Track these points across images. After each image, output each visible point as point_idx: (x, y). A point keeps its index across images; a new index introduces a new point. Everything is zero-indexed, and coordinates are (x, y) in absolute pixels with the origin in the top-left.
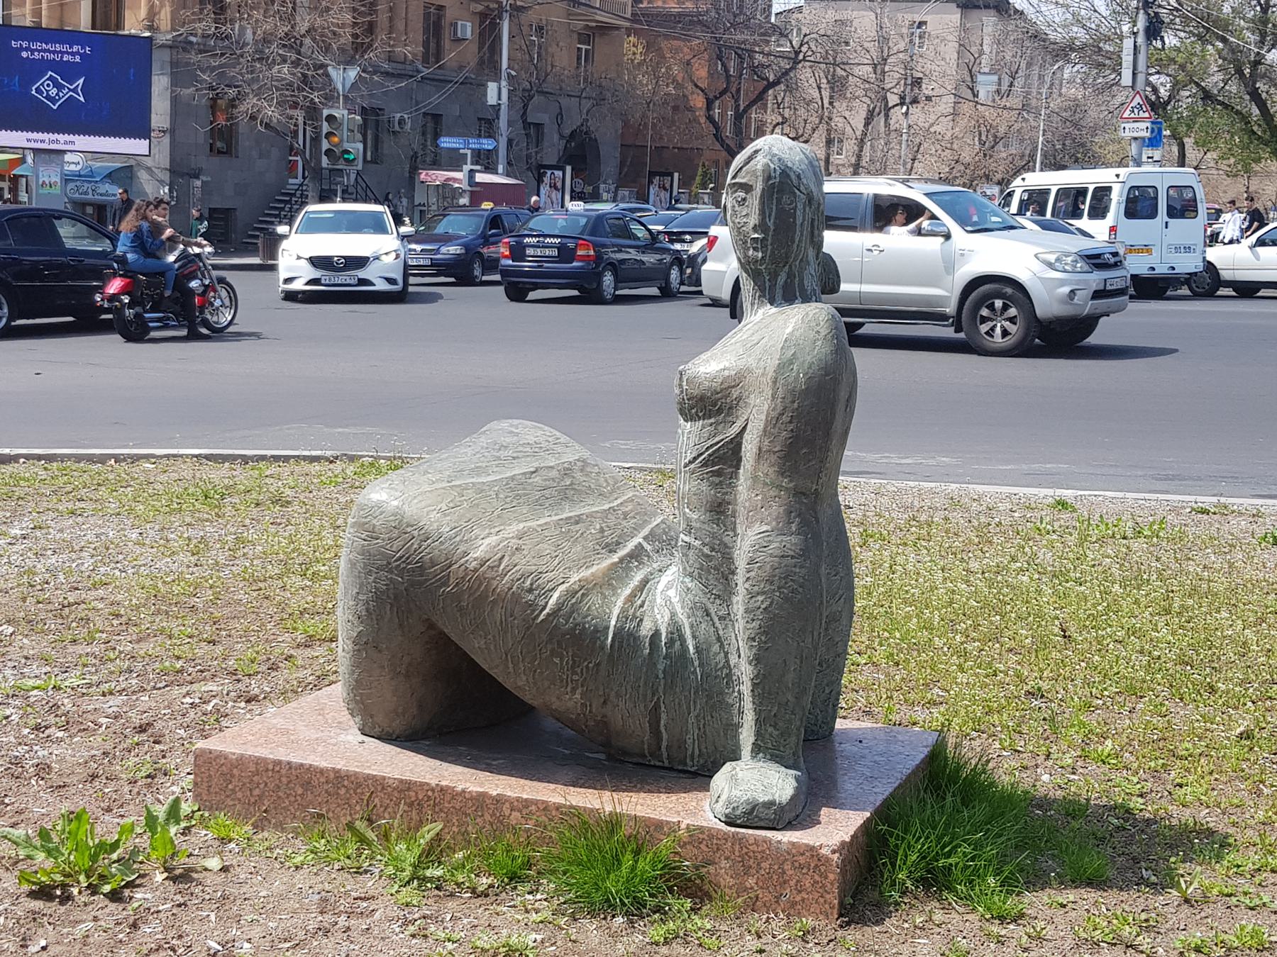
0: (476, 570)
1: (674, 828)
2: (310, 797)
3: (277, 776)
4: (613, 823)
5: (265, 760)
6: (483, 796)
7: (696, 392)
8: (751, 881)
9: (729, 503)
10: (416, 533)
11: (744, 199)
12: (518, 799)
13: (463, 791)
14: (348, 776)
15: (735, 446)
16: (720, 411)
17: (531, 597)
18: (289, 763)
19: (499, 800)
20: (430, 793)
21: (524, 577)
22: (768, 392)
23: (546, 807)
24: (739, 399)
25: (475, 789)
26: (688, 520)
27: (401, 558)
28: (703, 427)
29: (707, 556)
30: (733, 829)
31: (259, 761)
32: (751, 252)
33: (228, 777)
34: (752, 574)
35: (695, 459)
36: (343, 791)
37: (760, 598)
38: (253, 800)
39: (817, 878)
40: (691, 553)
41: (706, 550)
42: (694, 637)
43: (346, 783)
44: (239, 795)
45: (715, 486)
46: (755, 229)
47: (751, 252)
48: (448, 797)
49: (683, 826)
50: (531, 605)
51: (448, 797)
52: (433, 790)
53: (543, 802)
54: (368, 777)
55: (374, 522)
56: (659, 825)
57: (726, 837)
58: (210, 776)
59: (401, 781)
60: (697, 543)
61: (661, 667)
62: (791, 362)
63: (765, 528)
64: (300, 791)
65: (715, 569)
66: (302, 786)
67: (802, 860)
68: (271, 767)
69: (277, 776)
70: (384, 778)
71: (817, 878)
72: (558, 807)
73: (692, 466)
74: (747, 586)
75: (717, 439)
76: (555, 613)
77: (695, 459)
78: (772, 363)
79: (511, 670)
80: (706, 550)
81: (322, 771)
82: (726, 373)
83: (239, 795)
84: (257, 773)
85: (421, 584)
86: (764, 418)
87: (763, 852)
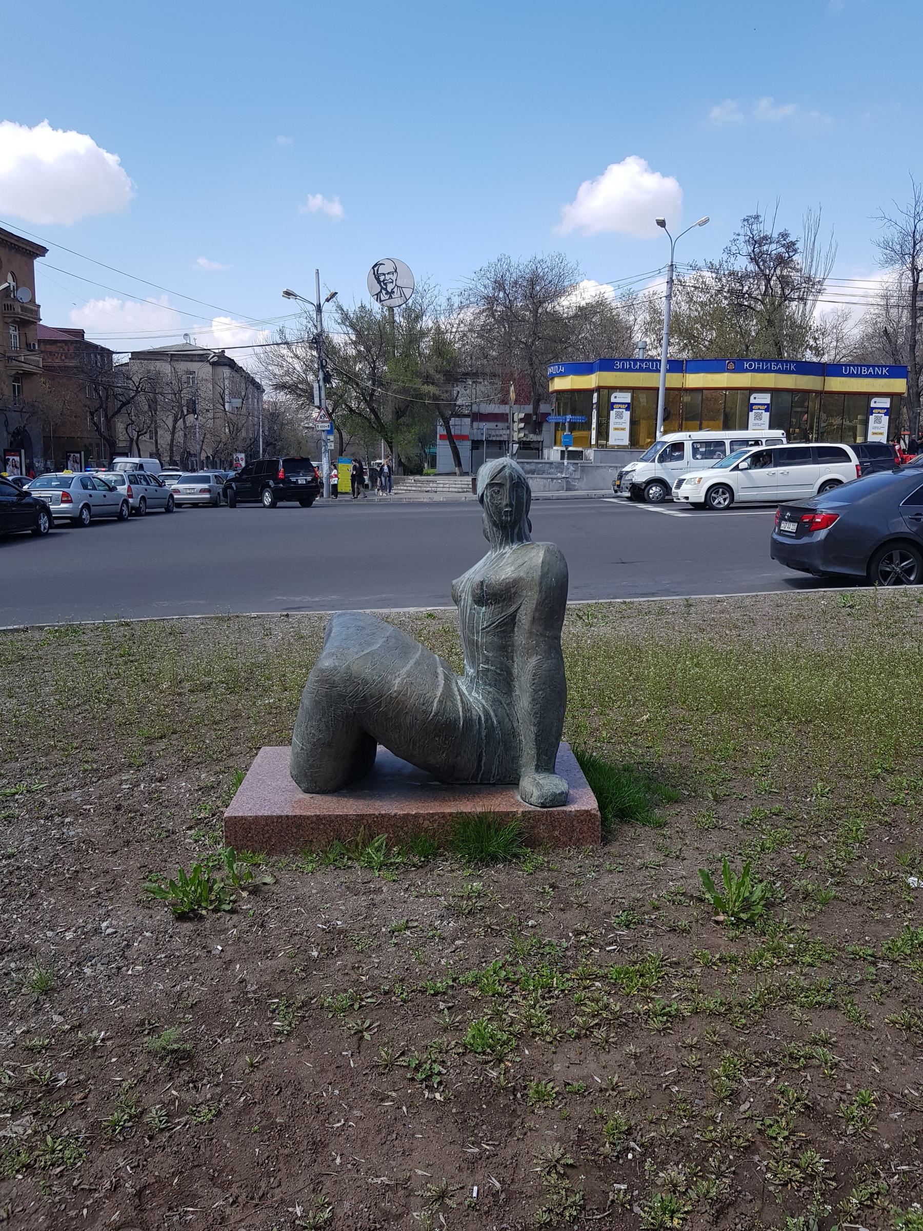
1: (514, 814)
4: (482, 817)
5: (271, 817)
6: (408, 814)
12: (427, 814)
13: (395, 815)
14: (325, 817)
15: (513, 616)
17: (424, 707)
18: (287, 816)
19: (416, 816)
21: (420, 696)
22: (537, 588)
23: (444, 815)
24: (515, 593)
26: (487, 657)
31: (267, 818)
36: (322, 827)
40: (489, 673)
41: (498, 671)
48: (386, 819)
50: (425, 712)
51: (386, 819)
56: (507, 814)
57: (543, 814)
61: (484, 734)
62: (547, 573)
64: (295, 830)
65: (501, 680)
72: (451, 814)
76: (436, 714)
78: (537, 574)
80: (498, 671)
81: (308, 818)
86: (535, 602)
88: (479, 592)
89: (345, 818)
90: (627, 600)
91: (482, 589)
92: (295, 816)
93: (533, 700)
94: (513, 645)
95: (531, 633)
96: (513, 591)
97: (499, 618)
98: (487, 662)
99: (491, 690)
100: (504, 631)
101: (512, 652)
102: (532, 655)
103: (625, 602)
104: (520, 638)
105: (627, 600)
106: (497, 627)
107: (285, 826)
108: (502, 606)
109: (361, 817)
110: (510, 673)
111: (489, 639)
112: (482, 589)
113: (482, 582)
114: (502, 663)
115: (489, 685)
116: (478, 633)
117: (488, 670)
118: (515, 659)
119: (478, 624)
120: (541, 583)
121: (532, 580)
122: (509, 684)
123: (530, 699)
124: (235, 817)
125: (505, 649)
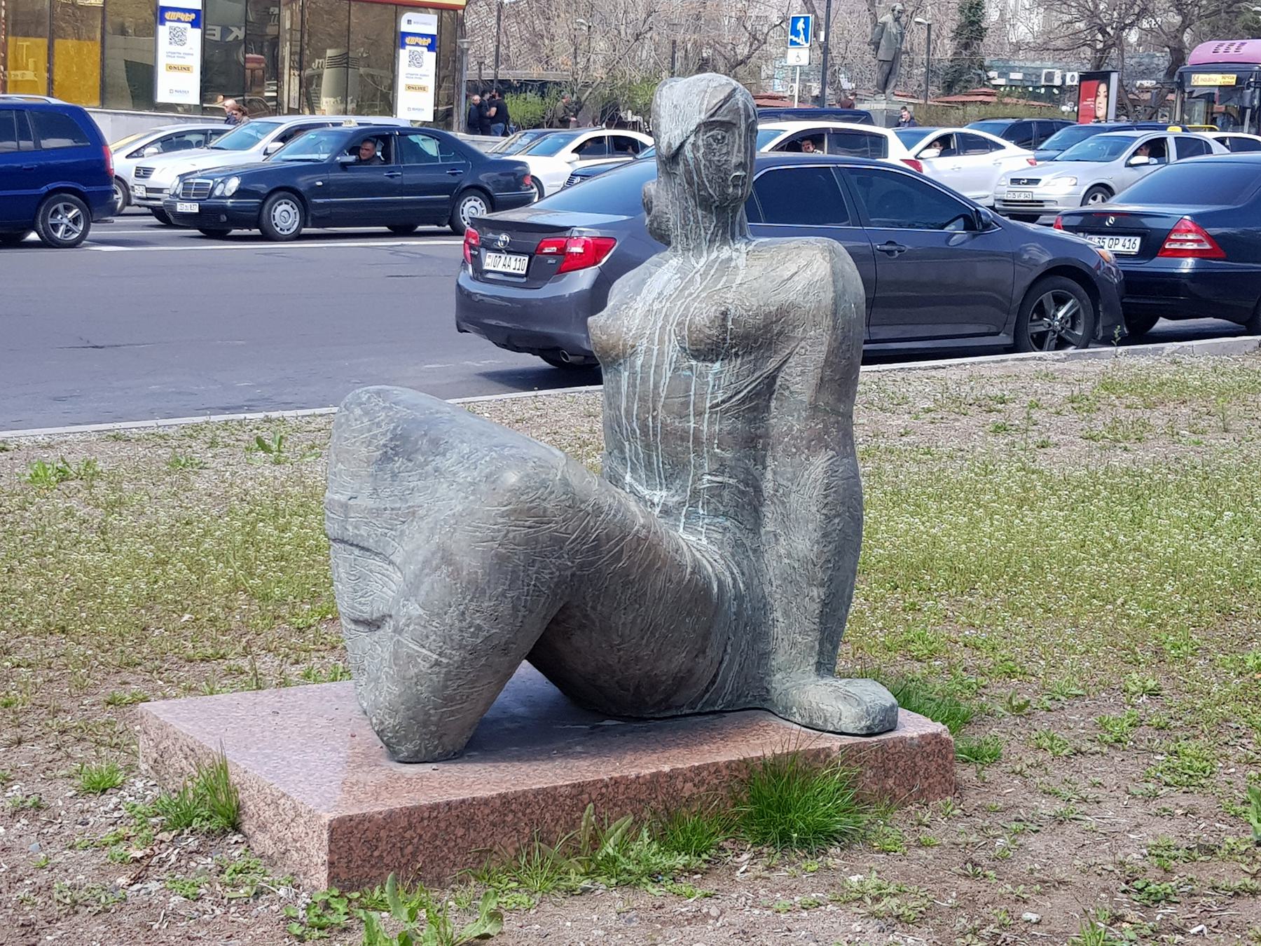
0: (647, 538)
2: (473, 834)
3: (433, 823)
5: (419, 809)
7: (741, 331)
8: (891, 782)
9: (760, 437)
10: (590, 509)
11: (724, 138)
12: (691, 769)
13: (638, 777)
16: (760, 347)
18: (448, 804)
19: (672, 775)
20: (604, 790)
22: (827, 322)
23: (716, 769)
24: (780, 333)
25: (647, 772)
27: (576, 539)
28: (742, 365)
29: (743, 492)
30: (874, 739)
31: (409, 812)
32: (731, 190)
33: (372, 844)
34: (830, 499)
35: (731, 397)
36: (510, 818)
37: (837, 521)
38: (404, 861)
39: (940, 761)
40: (726, 493)
41: (741, 487)
42: (743, 574)
43: (513, 807)
44: (388, 860)
45: (750, 421)
46: (738, 167)
47: (731, 190)
48: (622, 788)
49: (835, 749)
51: (622, 788)
52: (607, 786)
53: (714, 764)
54: (537, 793)
55: (545, 504)
58: (351, 848)
59: (574, 786)
60: (731, 481)
63: (831, 453)
64: (460, 832)
66: (463, 825)
67: (928, 749)
68: (426, 815)
69: (433, 823)
70: (555, 788)
71: (940, 761)
72: (728, 765)
73: (727, 405)
75: (756, 375)
77: (731, 397)
79: (644, 642)
80: (741, 487)
81: (486, 802)
82: (767, 309)
83: (388, 860)
84: (410, 826)
85: (592, 564)
86: (825, 348)
87: (900, 752)
88: (714, 332)
89: (549, 796)
90: (274, 415)
91: (723, 326)
92: (463, 801)
93: (825, 536)
94: (766, 435)
95: (814, 408)
96: (776, 329)
97: (748, 385)
98: (721, 468)
99: (728, 524)
100: (755, 409)
101: (764, 449)
102: (814, 453)
103: (268, 420)
104: (787, 420)
105: (274, 415)
106: (743, 401)
107: (443, 825)
108: (756, 360)
109: (580, 788)
110: (758, 490)
111: (727, 425)
112: (723, 326)
113: (725, 314)
114: (747, 471)
116: (699, 414)
117: (723, 485)
118: (769, 461)
119: (702, 396)
120: (835, 313)
121: (818, 309)
122: (756, 510)
125: (753, 442)
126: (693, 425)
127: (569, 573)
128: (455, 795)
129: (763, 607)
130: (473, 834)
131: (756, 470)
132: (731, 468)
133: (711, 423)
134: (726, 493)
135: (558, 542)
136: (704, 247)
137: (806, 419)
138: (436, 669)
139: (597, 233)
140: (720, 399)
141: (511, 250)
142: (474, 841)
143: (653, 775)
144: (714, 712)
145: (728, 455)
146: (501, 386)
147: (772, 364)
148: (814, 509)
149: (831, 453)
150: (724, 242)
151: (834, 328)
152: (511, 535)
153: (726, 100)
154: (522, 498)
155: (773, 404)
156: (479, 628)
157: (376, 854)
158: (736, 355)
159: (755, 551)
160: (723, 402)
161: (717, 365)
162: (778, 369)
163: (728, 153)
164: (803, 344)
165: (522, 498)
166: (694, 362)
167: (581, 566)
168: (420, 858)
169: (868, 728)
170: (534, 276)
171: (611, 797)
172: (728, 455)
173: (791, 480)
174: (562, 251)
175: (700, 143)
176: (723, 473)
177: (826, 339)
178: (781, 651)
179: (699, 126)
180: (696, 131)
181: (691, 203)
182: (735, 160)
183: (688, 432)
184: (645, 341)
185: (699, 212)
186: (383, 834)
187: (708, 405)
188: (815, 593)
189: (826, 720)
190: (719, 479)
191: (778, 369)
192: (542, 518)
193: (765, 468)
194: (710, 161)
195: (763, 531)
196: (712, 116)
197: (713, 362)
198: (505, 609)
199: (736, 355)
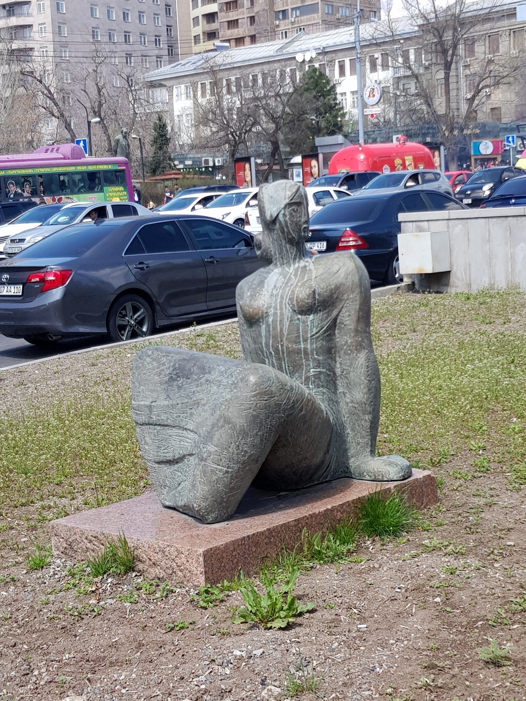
2: (259, 550)
3: (244, 546)
16: (329, 306)
18: (248, 536)
19: (332, 510)
22: (358, 290)
23: (348, 504)
24: (337, 298)
25: (322, 510)
26: (319, 361)
28: (323, 315)
29: (329, 375)
30: (406, 481)
32: (303, 234)
35: (319, 331)
36: (272, 540)
40: (322, 376)
41: (328, 372)
46: (304, 223)
49: (392, 488)
54: (282, 525)
55: (271, 389)
58: (212, 564)
59: (295, 521)
63: (367, 351)
69: (244, 546)
70: (288, 522)
73: (318, 335)
74: (368, 378)
77: (319, 331)
80: (328, 372)
81: (262, 533)
83: (227, 567)
84: (234, 550)
86: (358, 302)
88: (310, 301)
91: (314, 297)
93: (369, 390)
94: (336, 347)
95: (356, 331)
97: (326, 324)
99: (324, 391)
100: (329, 335)
101: (335, 353)
102: (358, 351)
104: (344, 338)
106: (325, 331)
107: (247, 547)
109: (297, 521)
110: (334, 373)
111: (319, 344)
112: (314, 297)
113: (314, 292)
115: (322, 386)
116: (305, 340)
118: (338, 359)
119: (306, 332)
120: (360, 286)
121: (352, 284)
122: (335, 383)
123: (365, 390)
124: (211, 549)
125: (330, 351)
126: (302, 346)
127: (283, 420)
128: (251, 532)
129: (343, 428)
130: (259, 550)
131: (332, 363)
132: (323, 364)
133: (312, 344)
134: (322, 376)
135: (278, 405)
136: (291, 261)
137: (354, 337)
138: (226, 475)
139: (60, 268)
140: (314, 333)
141: (11, 282)
142: (260, 553)
143: (325, 511)
144: (326, 482)
145: (321, 358)
146: (11, 359)
147: (335, 313)
148: (363, 378)
149: (367, 351)
150: (300, 259)
151: (361, 292)
152: (258, 405)
153: (297, 192)
154: (262, 387)
155: (336, 332)
156: (246, 452)
157: (223, 565)
158: (320, 310)
159: (336, 402)
160: (316, 333)
161: (311, 317)
162: (338, 315)
163: (300, 217)
164: (348, 302)
165: (262, 387)
166: (300, 316)
167: (287, 416)
168: (240, 564)
169: (403, 476)
170: (26, 295)
171: (312, 522)
172: (321, 358)
173: (350, 367)
174: (43, 280)
175: (287, 213)
176: (319, 367)
177: (358, 298)
178: (352, 448)
179: (286, 205)
180: (285, 208)
181: (284, 242)
182: (303, 220)
183: (301, 350)
184: (272, 309)
185: (288, 246)
186: (224, 555)
187: (309, 336)
188: (367, 418)
189: (383, 476)
190: (318, 370)
191: (338, 315)
192: (271, 394)
193: (336, 362)
194: (292, 221)
195: (338, 392)
196: (292, 200)
197: (309, 315)
198: (257, 441)
199: (320, 310)
